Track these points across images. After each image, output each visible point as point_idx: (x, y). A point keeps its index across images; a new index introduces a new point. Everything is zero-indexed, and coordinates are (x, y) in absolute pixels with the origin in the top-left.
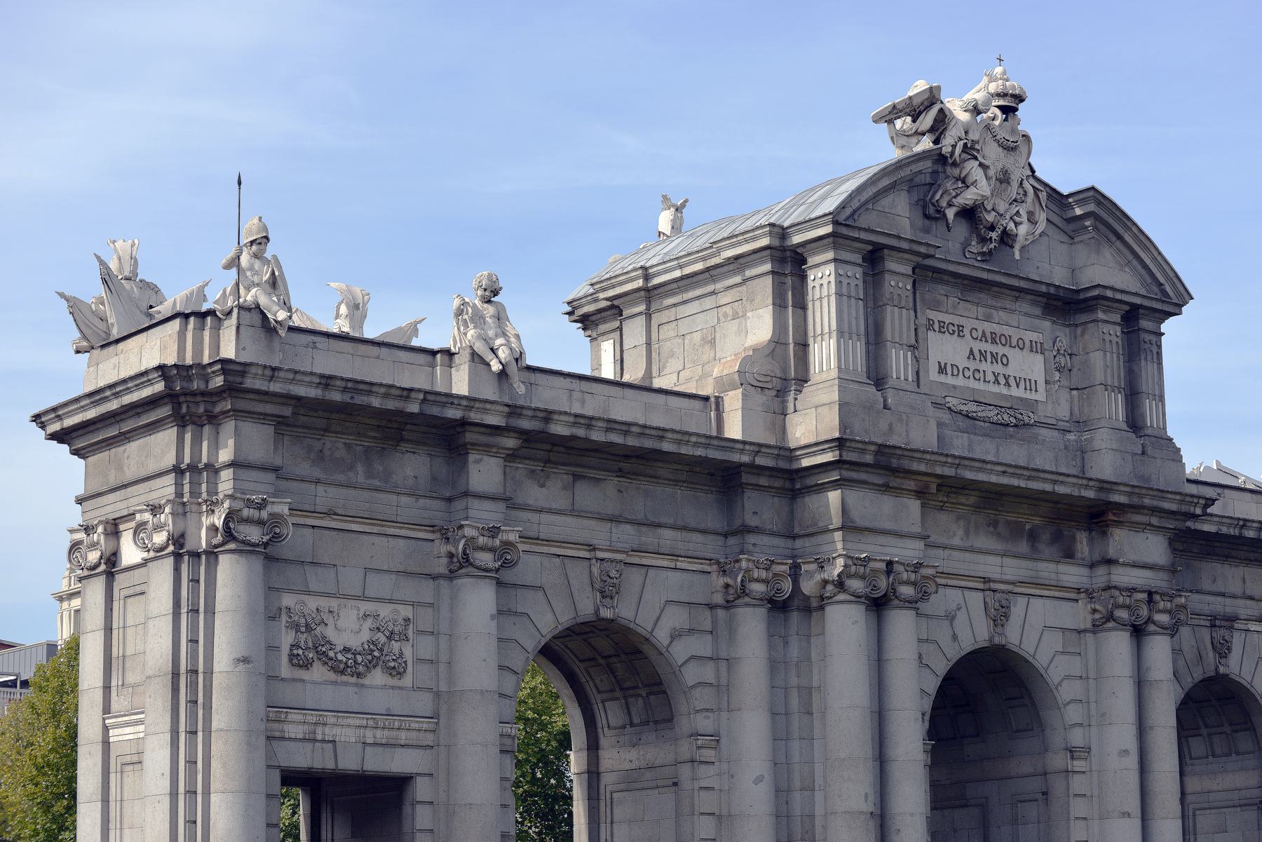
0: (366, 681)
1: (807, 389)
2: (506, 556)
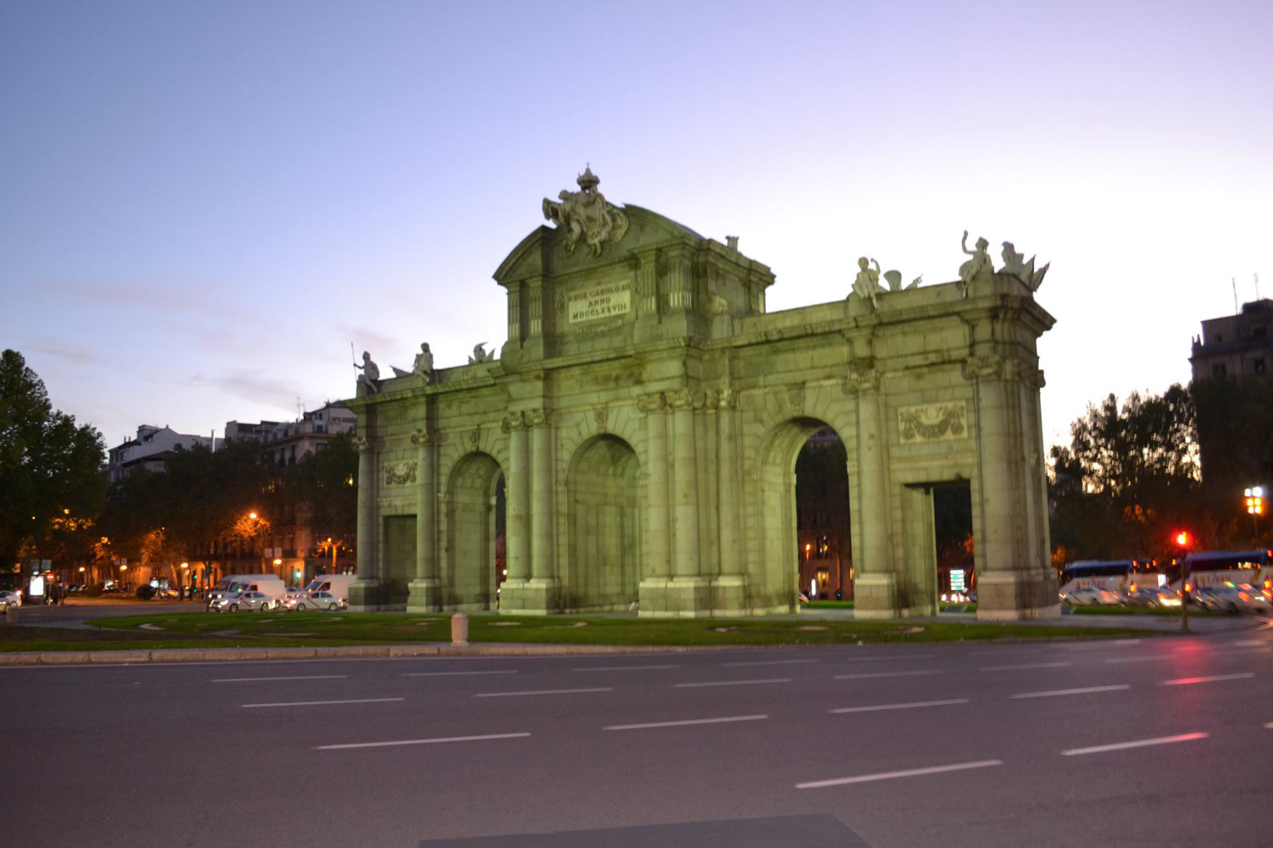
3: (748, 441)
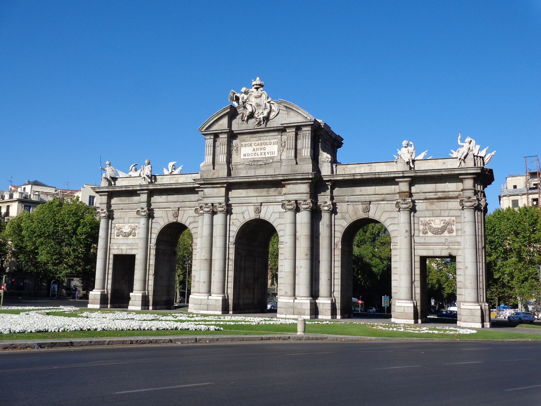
0: (129, 238)
3: (337, 228)
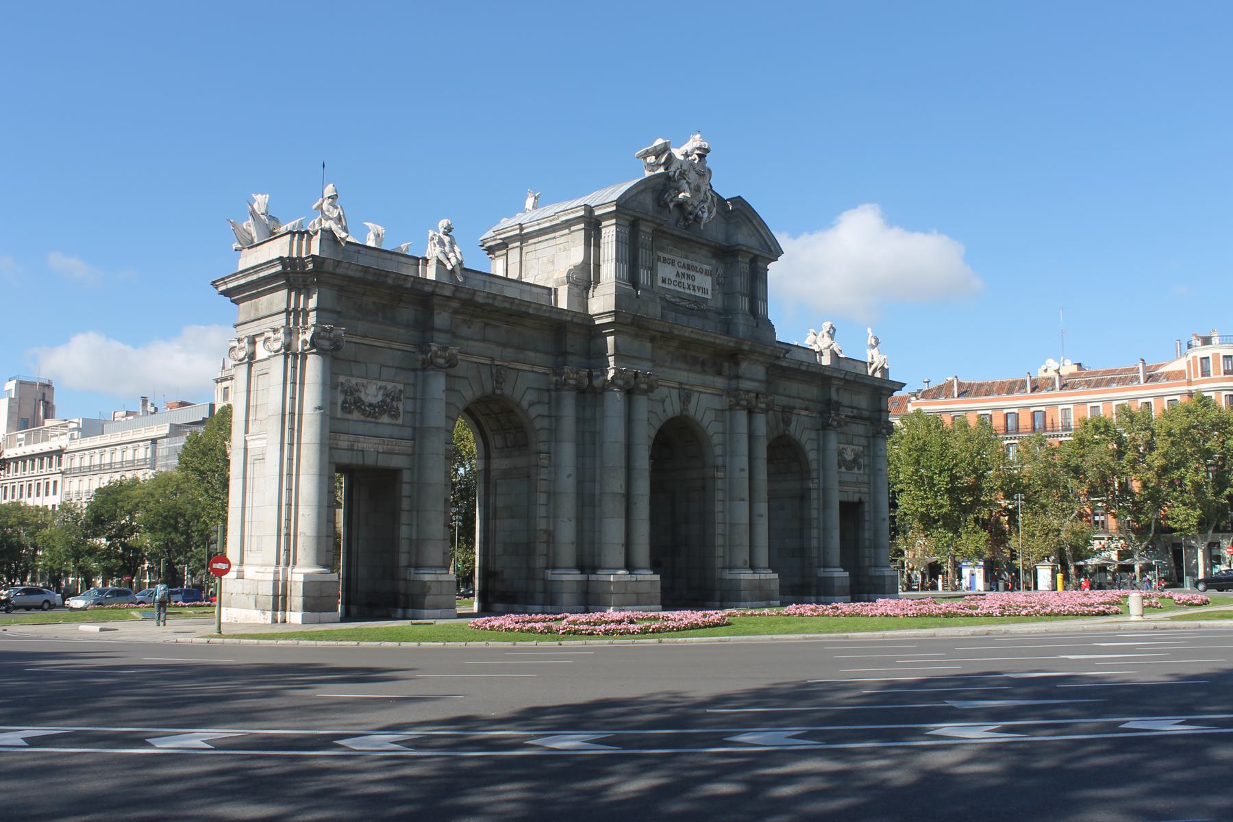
1: (599, 287)
2: (451, 363)
